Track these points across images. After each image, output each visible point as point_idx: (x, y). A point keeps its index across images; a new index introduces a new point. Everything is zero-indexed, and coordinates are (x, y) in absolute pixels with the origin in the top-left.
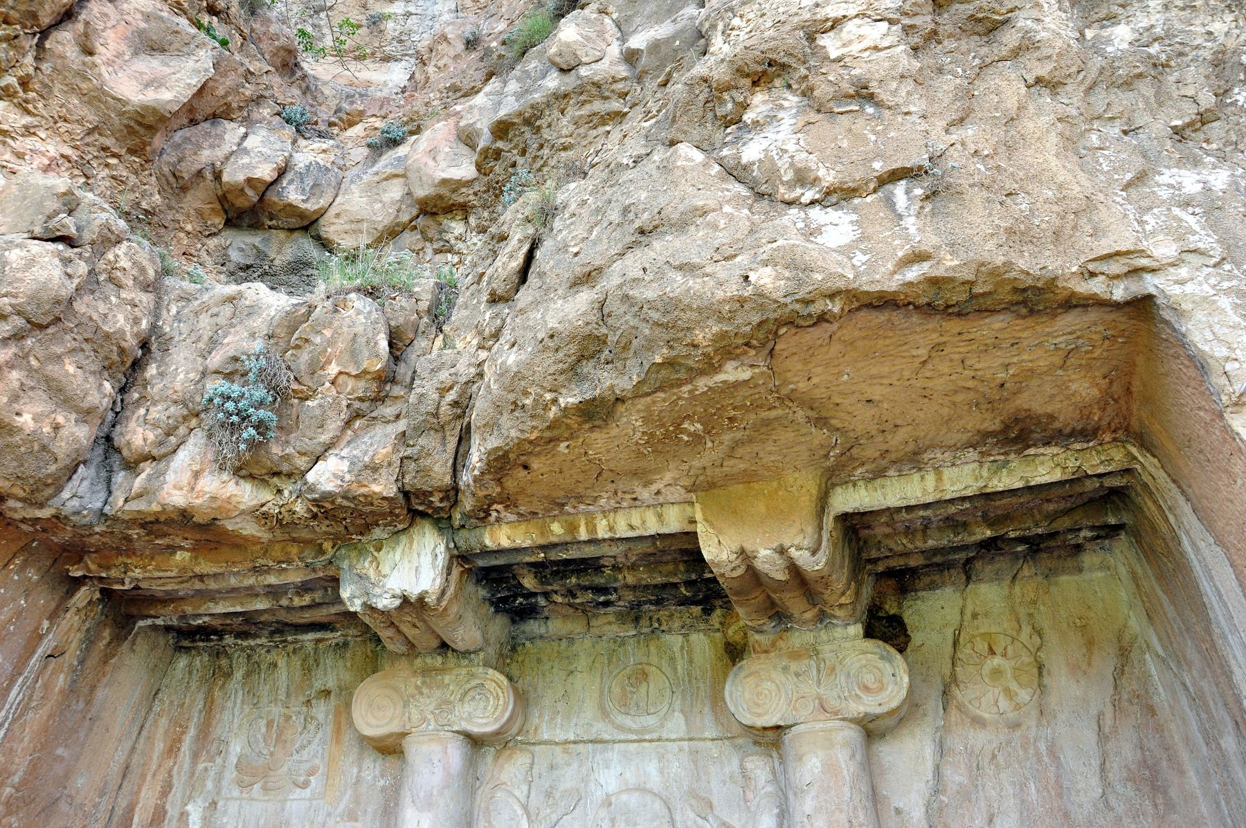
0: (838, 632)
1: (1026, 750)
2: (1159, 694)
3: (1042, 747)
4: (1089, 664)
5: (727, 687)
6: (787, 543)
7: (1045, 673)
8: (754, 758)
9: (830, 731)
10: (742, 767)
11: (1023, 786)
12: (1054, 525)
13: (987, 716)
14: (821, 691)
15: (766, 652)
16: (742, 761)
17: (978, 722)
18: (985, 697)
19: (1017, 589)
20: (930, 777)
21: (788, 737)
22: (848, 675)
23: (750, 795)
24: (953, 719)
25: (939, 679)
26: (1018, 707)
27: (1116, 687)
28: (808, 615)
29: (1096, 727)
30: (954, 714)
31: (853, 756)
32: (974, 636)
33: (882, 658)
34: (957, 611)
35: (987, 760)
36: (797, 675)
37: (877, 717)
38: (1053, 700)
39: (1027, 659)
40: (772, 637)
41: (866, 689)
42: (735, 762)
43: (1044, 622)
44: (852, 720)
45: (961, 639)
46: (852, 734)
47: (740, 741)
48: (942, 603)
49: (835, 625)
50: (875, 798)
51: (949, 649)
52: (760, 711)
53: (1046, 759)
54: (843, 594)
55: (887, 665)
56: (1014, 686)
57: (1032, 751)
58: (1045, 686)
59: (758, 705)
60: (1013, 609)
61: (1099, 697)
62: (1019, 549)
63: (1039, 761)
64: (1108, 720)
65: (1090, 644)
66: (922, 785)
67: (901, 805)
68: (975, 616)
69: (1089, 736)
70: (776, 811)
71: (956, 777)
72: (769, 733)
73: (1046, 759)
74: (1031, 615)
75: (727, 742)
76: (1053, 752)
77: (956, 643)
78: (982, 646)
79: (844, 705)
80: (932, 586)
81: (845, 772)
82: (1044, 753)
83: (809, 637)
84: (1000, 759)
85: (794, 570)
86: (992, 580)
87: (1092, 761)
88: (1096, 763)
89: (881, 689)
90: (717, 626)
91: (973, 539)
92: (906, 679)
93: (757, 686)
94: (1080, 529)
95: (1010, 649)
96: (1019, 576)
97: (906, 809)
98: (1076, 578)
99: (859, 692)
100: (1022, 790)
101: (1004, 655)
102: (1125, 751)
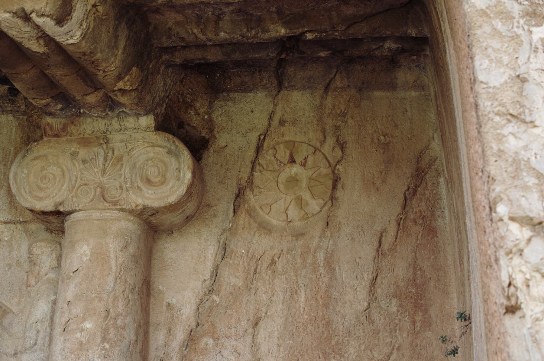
0: (131, 122)
1: (304, 260)
2: (444, 217)
3: (321, 257)
4: (384, 182)
5: (13, 169)
6: (28, 7)
7: (339, 186)
8: (42, 244)
9: (106, 220)
10: (30, 252)
11: (294, 292)
12: (351, 31)
13: (275, 222)
14: (105, 180)
15: (57, 136)
16: (30, 246)
17: (265, 228)
18: (275, 202)
19: (329, 101)
20: (208, 276)
21: (67, 224)
22: (134, 166)
23: (32, 281)
24: (241, 222)
25: (235, 181)
26: (306, 217)
27: (404, 207)
28: (92, 99)
29: (376, 244)
30: (243, 216)
31: (126, 247)
32: (278, 143)
33: (169, 152)
34: (265, 116)
35: (265, 265)
36: (84, 162)
37: (156, 212)
38: (341, 213)
39: (325, 170)
40: (63, 121)
41: (149, 181)
42: (25, 246)
43: (349, 136)
44: (131, 212)
45: (265, 145)
46: (129, 226)
47: (33, 226)
48: (252, 106)
49: (129, 115)
50: (145, 291)
51: (251, 153)
52: (42, 195)
53: (321, 269)
54: (120, 78)
55: (173, 159)
56: (306, 196)
57: (310, 261)
58: (336, 199)
59: (41, 189)
60: (320, 120)
61: (386, 213)
62: (322, 54)
63: (315, 270)
64: (389, 239)
65: (389, 162)
66: (199, 284)
67: (174, 301)
68: (282, 123)
69: (368, 251)
70: (53, 297)
71: (232, 278)
72: (51, 218)
73: (321, 269)
74: (337, 128)
75: (19, 227)
76: (329, 264)
77: (259, 148)
78: (283, 154)
79: (124, 195)
80: (244, 89)
81: (113, 262)
82: (321, 264)
83: (101, 125)
84: (279, 266)
85: (48, 40)
86: (303, 88)
87: (366, 276)
88: (368, 277)
89: (163, 182)
90: (23, 107)
91: (267, 36)
92: (189, 176)
93: (43, 169)
94: (384, 39)
95: (310, 160)
96: (332, 86)
97: (179, 305)
98: (389, 94)
99: (140, 184)
100: (292, 296)
101: (304, 165)
102: (399, 269)
